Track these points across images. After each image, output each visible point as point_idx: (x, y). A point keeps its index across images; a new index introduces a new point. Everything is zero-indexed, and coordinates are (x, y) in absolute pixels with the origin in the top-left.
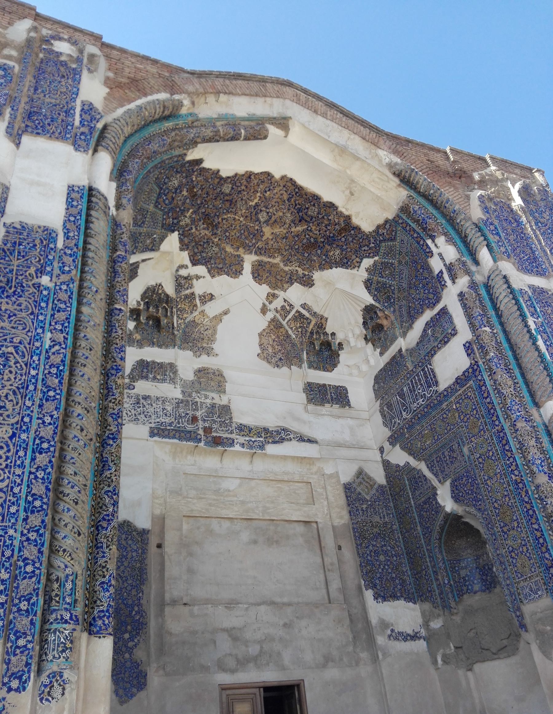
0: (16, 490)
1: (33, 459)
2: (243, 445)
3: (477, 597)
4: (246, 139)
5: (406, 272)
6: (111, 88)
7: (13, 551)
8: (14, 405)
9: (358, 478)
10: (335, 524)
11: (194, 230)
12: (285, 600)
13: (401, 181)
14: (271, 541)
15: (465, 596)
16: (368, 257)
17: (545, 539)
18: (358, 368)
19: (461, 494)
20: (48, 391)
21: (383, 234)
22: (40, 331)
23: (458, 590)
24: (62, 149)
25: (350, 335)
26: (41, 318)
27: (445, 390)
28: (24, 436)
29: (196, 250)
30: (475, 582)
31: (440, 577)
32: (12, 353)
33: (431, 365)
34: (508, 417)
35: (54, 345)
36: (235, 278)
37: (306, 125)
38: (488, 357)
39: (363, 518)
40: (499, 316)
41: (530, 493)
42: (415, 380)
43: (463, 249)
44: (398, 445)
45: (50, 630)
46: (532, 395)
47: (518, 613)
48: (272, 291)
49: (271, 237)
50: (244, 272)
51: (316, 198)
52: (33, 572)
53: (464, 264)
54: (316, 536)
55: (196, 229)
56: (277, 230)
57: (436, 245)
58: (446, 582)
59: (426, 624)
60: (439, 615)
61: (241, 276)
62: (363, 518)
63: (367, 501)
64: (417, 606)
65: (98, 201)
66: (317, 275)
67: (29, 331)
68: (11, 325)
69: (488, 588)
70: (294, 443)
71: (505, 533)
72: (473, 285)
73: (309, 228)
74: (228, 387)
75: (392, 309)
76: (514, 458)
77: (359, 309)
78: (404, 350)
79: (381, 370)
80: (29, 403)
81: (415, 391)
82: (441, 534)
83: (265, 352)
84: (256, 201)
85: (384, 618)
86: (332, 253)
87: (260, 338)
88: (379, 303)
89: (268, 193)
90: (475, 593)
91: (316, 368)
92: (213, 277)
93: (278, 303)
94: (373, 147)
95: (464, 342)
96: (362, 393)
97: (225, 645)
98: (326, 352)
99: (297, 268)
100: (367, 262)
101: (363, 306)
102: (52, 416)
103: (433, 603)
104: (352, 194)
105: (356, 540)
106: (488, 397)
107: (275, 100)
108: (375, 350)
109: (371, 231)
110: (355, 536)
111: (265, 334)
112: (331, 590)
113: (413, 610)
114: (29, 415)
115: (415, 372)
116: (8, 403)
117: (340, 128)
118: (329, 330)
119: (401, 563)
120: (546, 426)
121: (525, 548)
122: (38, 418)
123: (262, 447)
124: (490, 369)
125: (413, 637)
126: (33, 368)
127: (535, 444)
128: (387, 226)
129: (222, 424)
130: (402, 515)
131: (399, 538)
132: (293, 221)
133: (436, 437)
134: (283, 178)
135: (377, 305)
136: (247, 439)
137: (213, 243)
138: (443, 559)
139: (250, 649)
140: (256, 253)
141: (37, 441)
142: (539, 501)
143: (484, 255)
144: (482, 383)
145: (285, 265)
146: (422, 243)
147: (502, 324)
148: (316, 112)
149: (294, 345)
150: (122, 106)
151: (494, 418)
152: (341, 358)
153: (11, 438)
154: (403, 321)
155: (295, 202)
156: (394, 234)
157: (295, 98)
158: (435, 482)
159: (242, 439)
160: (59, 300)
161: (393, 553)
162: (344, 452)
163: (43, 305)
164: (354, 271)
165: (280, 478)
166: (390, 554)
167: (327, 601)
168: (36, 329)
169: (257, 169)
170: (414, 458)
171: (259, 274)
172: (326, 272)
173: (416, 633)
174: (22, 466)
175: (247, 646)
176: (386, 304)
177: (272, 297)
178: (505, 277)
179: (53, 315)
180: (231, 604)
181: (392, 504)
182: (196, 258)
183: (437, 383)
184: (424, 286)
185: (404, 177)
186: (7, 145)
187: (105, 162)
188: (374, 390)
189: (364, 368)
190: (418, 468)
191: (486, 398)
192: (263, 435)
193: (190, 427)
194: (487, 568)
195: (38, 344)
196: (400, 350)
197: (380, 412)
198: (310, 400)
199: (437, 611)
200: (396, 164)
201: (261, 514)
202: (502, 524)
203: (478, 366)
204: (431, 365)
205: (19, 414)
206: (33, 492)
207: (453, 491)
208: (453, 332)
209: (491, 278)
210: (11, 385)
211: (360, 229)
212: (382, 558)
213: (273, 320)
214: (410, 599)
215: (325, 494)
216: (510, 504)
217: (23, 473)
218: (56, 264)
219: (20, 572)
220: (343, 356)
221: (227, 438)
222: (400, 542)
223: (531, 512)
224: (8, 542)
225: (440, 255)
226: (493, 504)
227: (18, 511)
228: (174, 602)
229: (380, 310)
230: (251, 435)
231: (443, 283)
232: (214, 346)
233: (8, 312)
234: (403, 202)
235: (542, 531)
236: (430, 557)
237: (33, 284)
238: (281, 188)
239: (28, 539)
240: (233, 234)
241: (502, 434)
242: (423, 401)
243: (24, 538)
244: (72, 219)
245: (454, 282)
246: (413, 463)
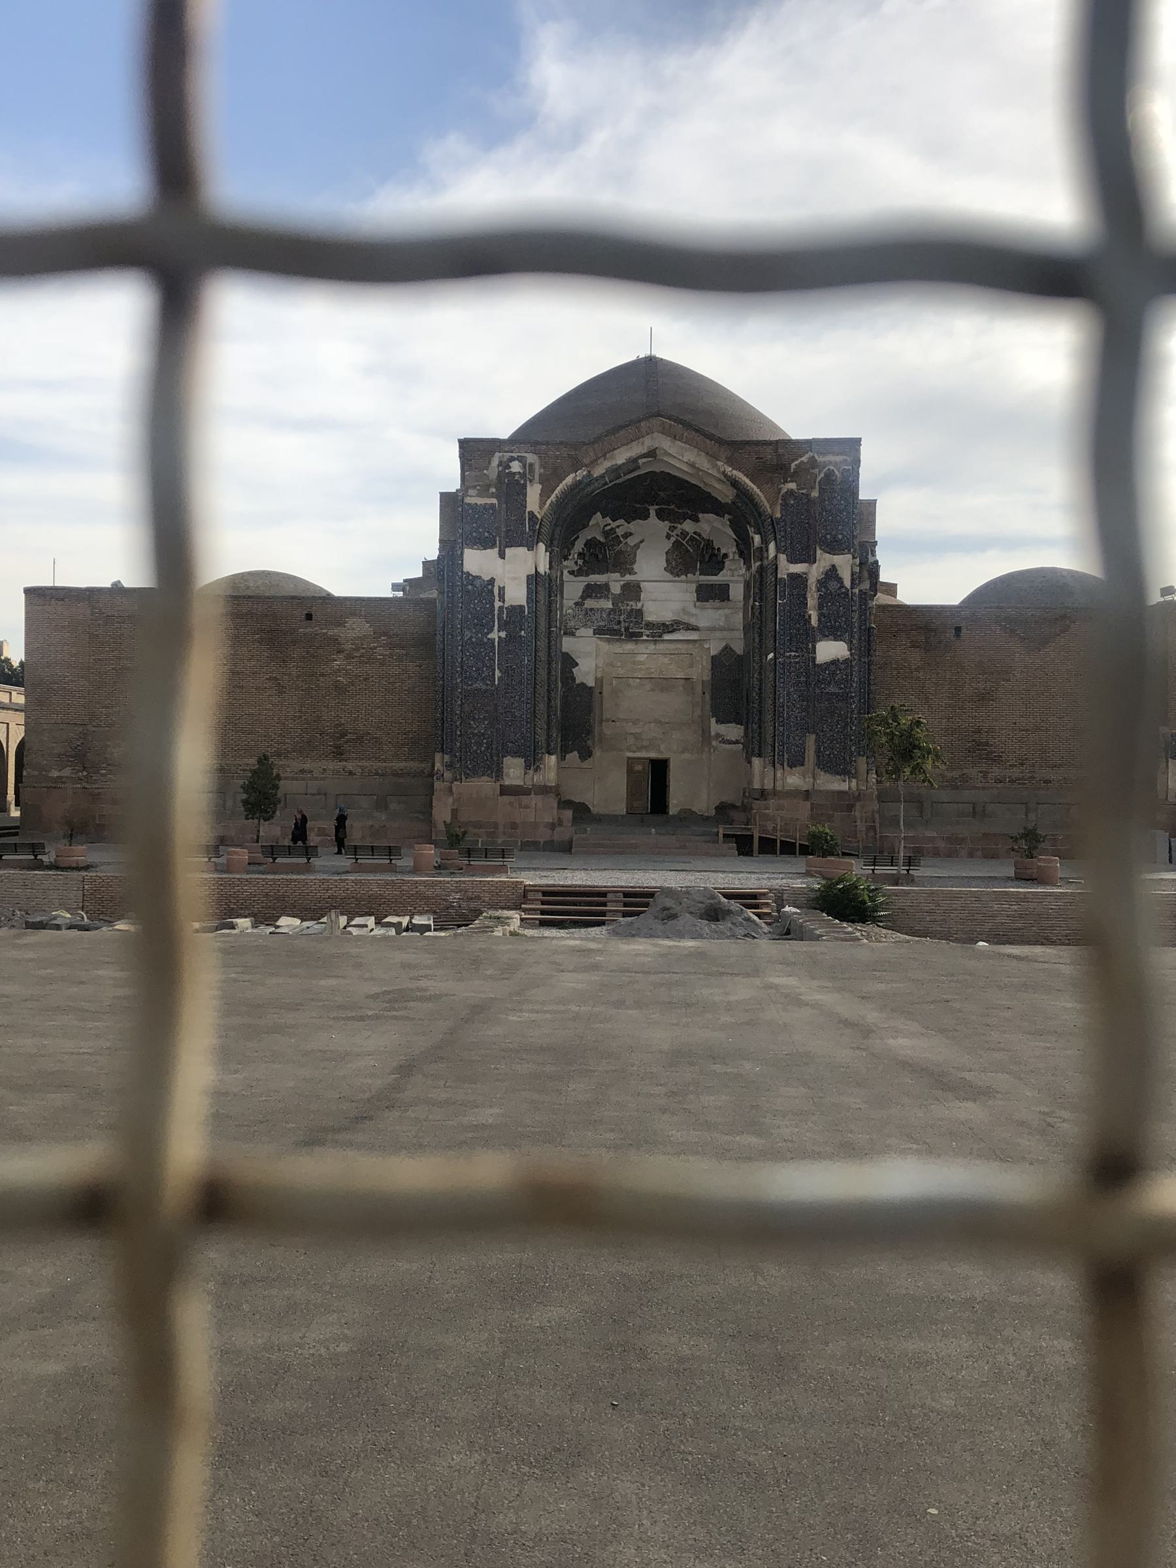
14: (662, 690)
24: (522, 551)
66: (700, 515)
74: (642, 595)
96: (737, 592)
97: (631, 740)
123: (660, 636)
129: (637, 623)
143: (772, 547)
162: (718, 634)
171: (660, 515)
177: (672, 529)
180: (635, 722)
186: (501, 561)
187: (542, 546)
193: (616, 627)
198: (698, 600)
220: (727, 563)
228: (607, 720)
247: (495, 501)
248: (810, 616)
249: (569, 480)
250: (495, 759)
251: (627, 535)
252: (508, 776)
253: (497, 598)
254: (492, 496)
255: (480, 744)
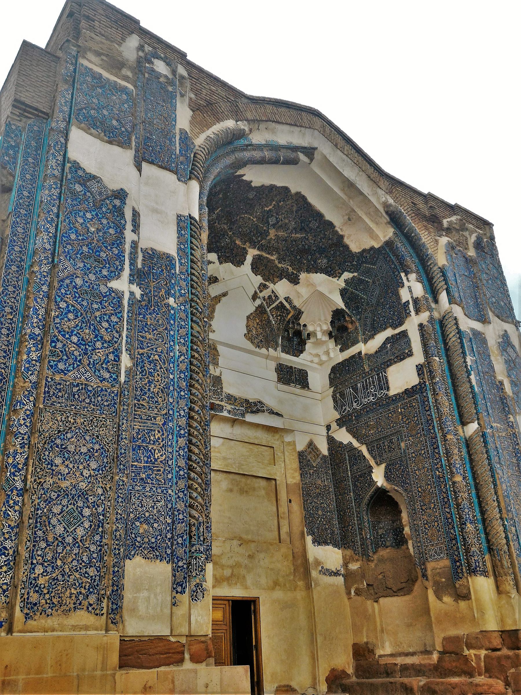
0: (170, 463)
1: (177, 441)
2: (229, 412)
3: (388, 550)
4: (283, 163)
5: (377, 292)
6: (193, 111)
7: (172, 504)
8: (163, 401)
9: (309, 448)
10: (289, 482)
11: (217, 224)
12: (249, 537)
13: (391, 219)
14: (243, 491)
15: (379, 549)
16: (350, 272)
17: (453, 520)
18: (320, 357)
19: (393, 476)
20: (181, 391)
21: (367, 257)
22: (172, 343)
23: (375, 544)
25: (318, 329)
26: (172, 333)
27: (394, 396)
28: (170, 424)
29: (214, 240)
30: (388, 539)
31: (363, 533)
32: (157, 360)
33: (385, 373)
34: (442, 429)
35: (181, 355)
36: (238, 266)
37: (328, 156)
38: (434, 381)
39: (310, 480)
40: (447, 350)
41: (448, 487)
42: (369, 381)
43: (428, 287)
44: (345, 427)
45: (192, 557)
46: (461, 416)
47: (423, 567)
48: (264, 282)
49: (273, 238)
50: (245, 263)
51: (319, 216)
52: (183, 519)
53: (427, 299)
54: (274, 491)
55: (219, 223)
56: (280, 234)
57: (407, 279)
58: (368, 537)
59: (345, 565)
60: (357, 560)
61: (242, 266)
62: (310, 480)
63: (314, 467)
64: (340, 551)
65: (196, 230)
66: (303, 276)
67: (165, 343)
68: (155, 337)
69: (397, 545)
70: (266, 413)
71: (423, 510)
72: (431, 319)
73: (307, 237)
74: (221, 361)
75: (358, 317)
76: (441, 460)
77: (331, 310)
78: (363, 354)
79: (339, 364)
80: (171, 400)
81: (367, 389)
82: (370, 501)
83: (251, 333)
84: (270, 207)
85: (318, 558)
86: (320, 261)
87: (248, 320)
88: (349, 309)
89: (282, 203)
90: (387, 547)
91: (287, 353)
92: (221, 263)
93: (266, 293)
94: (375, 185)
95: (417, 364)
96: (319, 379)
98: (296, 339)
99: (288, 267)
100: (347, 275)
101: (335, 309)
102: (184, 410)
103: (355, 551)
104: (349, 219)
105: (303, 496)
106: (429, 410)
107: (307, 129)
108: (336, 346)
109: (358, 250)
110: (303, 493)
111: (252, 318)
112: (281, 533)
113: (338, 553)
114: (172, 409)
115: (370, 374)
116: (159, 399)
117: (353, 163)
118: (302, 322)
119: (333, 518)
120: (466, 440)
121: (436, 523)
122: (177, 412)
123: (243, 415)
124: (434, 390)
125: (336, 573)
126: (171, 373)
127: (457, 453)
128: (372, 252)
130: (338, 483)
131: (333, 499)
132: (295, 229)
133: (380, 430)
134: (298, 194)
135: (347, 310)
136: (233, 407)
137: (227, 235)
138: (368, 520)
139: (225, 572)
140: (258, 249)
141: (178, 429)
142: (453, 493)
143: (443, 297)
144: (426, 399)
145: (279, 263)
146: (396, 273)
147: (448, 356)
148: (336, 146)
149: (272, 330)
150: (204, 131)
151: (431, 428)
152: (307, 346)
153: (164, 425)
154: (366, 330)
155: (301, 214)
156: (375, 259)
157: (322, 129)
158: (372, 463)
159: (229, 407)
160: (181, 318)
161: (328, 509)
163: (172, 322)
164: (335, 280)
165: (252, 441)
166: (326, 510)
167: (278, 541)
168: (170, 342)
169: (279, 184)
170: (358, 441)
171: (258, 266)
172: (311, 274)
173: (338, 571)
174: (171, 446)
175: (223, 569)
176: (354, 312)
177: (263, 287)
178: (456, 319)
179: (178, 331)
181: (330, 472)
182: (212, 246)
183: (388, 389)
184: (390, 308)
185: (395, 217)
188: (330, 378)
189: (324, 358)
190: (360, 449)
191: (427, 411)
192: (244, 405)
194: (398, 530)
195: (172, 354)
196: (361, 352)
197: (333, 397)
199: (357, 557)
200: (390, 205)
201: (237, 469)
202: (422, 504)
203: (425, 385)
204: (385, 373)
205: (166, 407)
206: (178, 465)
207: (386, 473)
208: (409, 353)
209: (446, 318)
210: (160, 385)
211: (348, 248)
212: (320, 512)
213: (260, 306)
214: (336, 545)
215: (283, 457)
216: (431, 491)
217: (173, 451)
218: (176, 288)
219: (176, 519)
220: (308, 346)
221: (218, 405)
222: (333, 502)
223: (446, 500)
224: (169, 498)
225: (409, 287)
226: (418, 488)
227: (172, 477)
229: (348, 315)
230: (236, 404)
231: (408, 312)
232: (212, 323)
233: (152, 326)
234: (390, 238)
235: (452, 514)
236: (357, 517)
237: (165, 304)
238: (293, 201)
239: (179, 497)
240: (245, 230)
241: (434, 440)
242: (373, 399)
243: (177, 496)
244: (182, 247)
245: (417, 313)
246: (356, 444)
247: (130, 86)
248: (501, 383)
249: (230, 124)
250: (110, 560)
251: (214, 280)
252: (133, 610)
253: (129, 227)
254: (126, 78)
255: (72, 519)
